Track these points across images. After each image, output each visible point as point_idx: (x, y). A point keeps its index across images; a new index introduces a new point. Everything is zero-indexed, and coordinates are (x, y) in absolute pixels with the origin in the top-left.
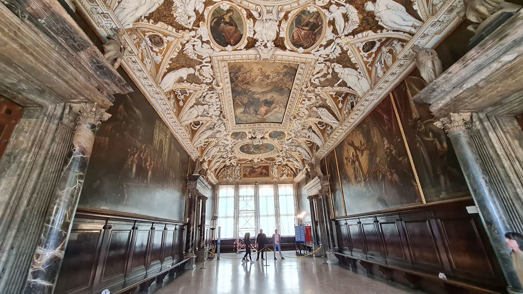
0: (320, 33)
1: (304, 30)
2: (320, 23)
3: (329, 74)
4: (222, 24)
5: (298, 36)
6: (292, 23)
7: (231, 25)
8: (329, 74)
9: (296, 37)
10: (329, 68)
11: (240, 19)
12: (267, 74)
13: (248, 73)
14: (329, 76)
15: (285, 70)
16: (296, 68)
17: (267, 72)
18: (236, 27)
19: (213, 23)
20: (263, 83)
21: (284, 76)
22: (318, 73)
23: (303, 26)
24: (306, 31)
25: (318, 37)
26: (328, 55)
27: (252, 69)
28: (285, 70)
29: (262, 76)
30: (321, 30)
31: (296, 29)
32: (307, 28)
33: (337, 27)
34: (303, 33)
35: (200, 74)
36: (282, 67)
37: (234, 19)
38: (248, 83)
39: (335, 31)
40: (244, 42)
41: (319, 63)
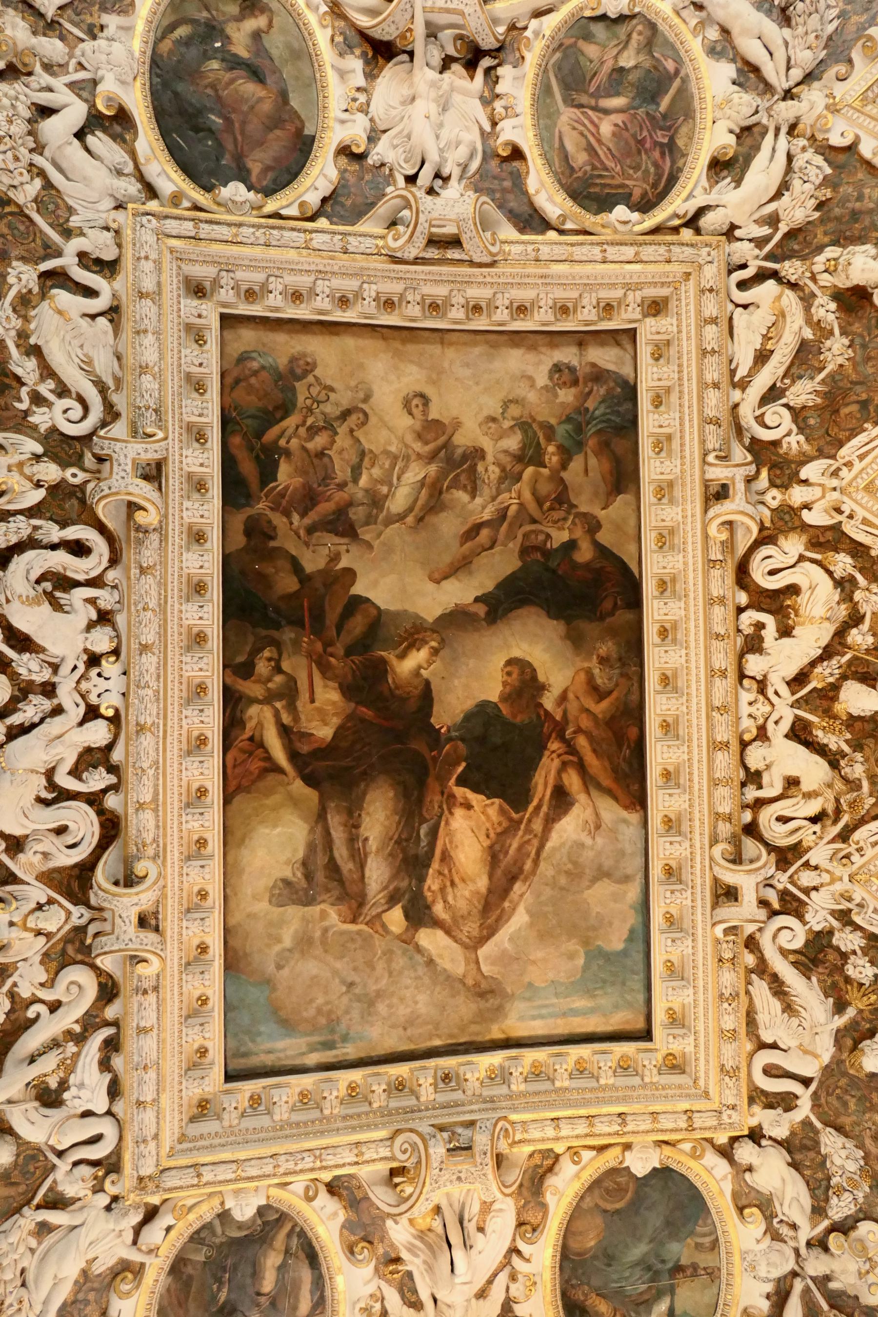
0: (685, 108)
1: (606, 112)
2: (670, 65)
3: (823, 332)
4: (215, 65)
5: (591, 150)
6: (547, 90)
7: (256, 74)
8: (823, 332)
9: (580, 159)
10: (807, 300)
11: (303, 53)
12: (462, 440)
13: (342, 430)
14: (837, 351)
15: (567, 396)
16: (626, 371)
17: (457, 425)
18: (283, 96)
19: (166, 46)
20: (449, 526)
21: (566, 455)
22: (762, 357)
23: (596, 95)
24: (618, 118)
25: (684, 130)
26: (773, 220)
27: (367, 399)
28: (567, 396)
29: (432, 457)
30: (683, 94)
31: (567, 115)
32: (618, 102)
33: (754, 51)
34: (606, 128)
35: (22, 335)
36: (542, 380)
37: (275, 53)
38: (341, 524)
39: (750, 74)
40: (321, 175)
41: (742, 285)
